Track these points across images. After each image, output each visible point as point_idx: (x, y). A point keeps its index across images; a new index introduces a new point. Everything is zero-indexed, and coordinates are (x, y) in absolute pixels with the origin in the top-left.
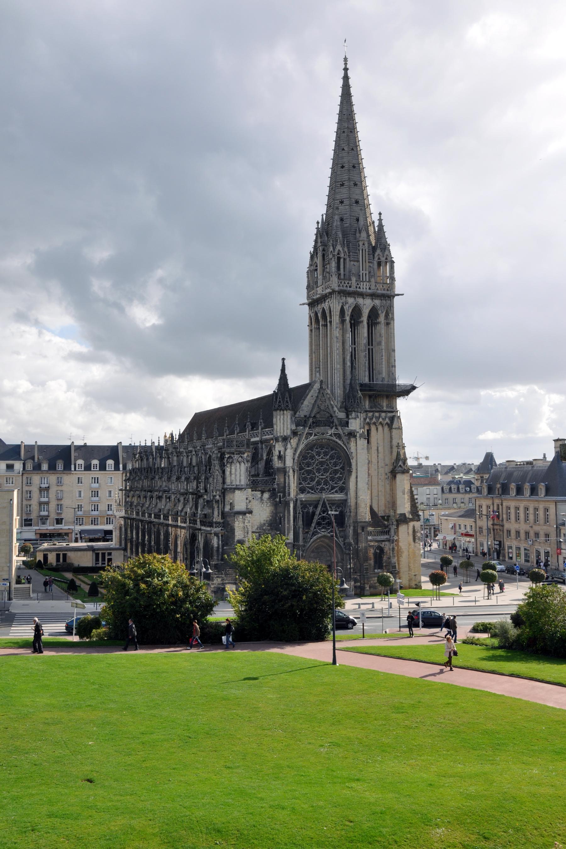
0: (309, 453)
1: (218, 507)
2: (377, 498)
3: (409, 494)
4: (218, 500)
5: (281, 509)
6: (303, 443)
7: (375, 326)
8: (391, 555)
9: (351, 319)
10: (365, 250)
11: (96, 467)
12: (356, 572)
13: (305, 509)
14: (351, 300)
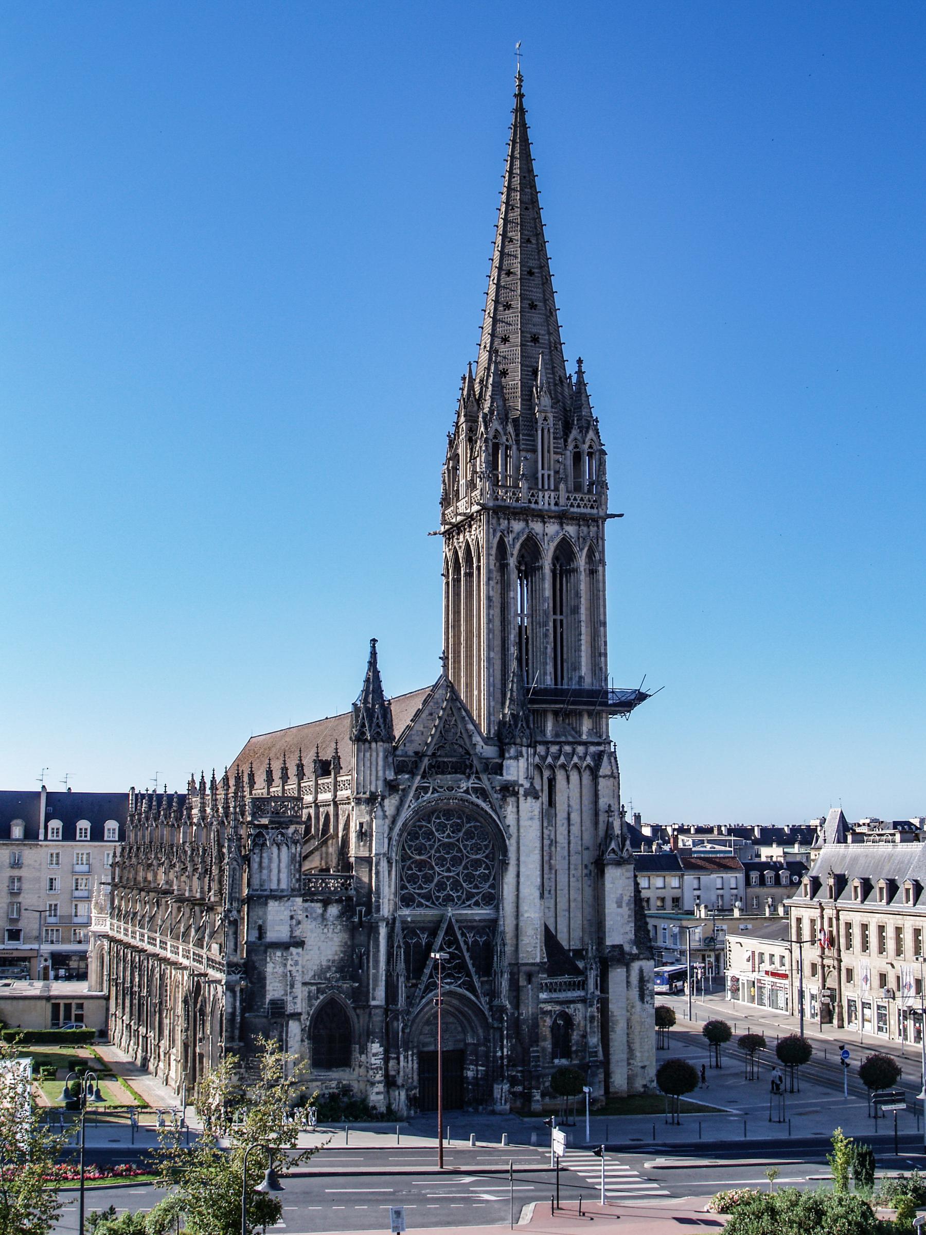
0: (422, 826)
2: (567, 913)
3: (633, 906)
5: (362, 938)
6: (409, 806)
7: (566, 576)
8: (588, 1030)
9: (519, 562)
10: (549, 430)
11: (86, 833)
12: (514, 1066)
13: (412, 939)
14: (517, 526)
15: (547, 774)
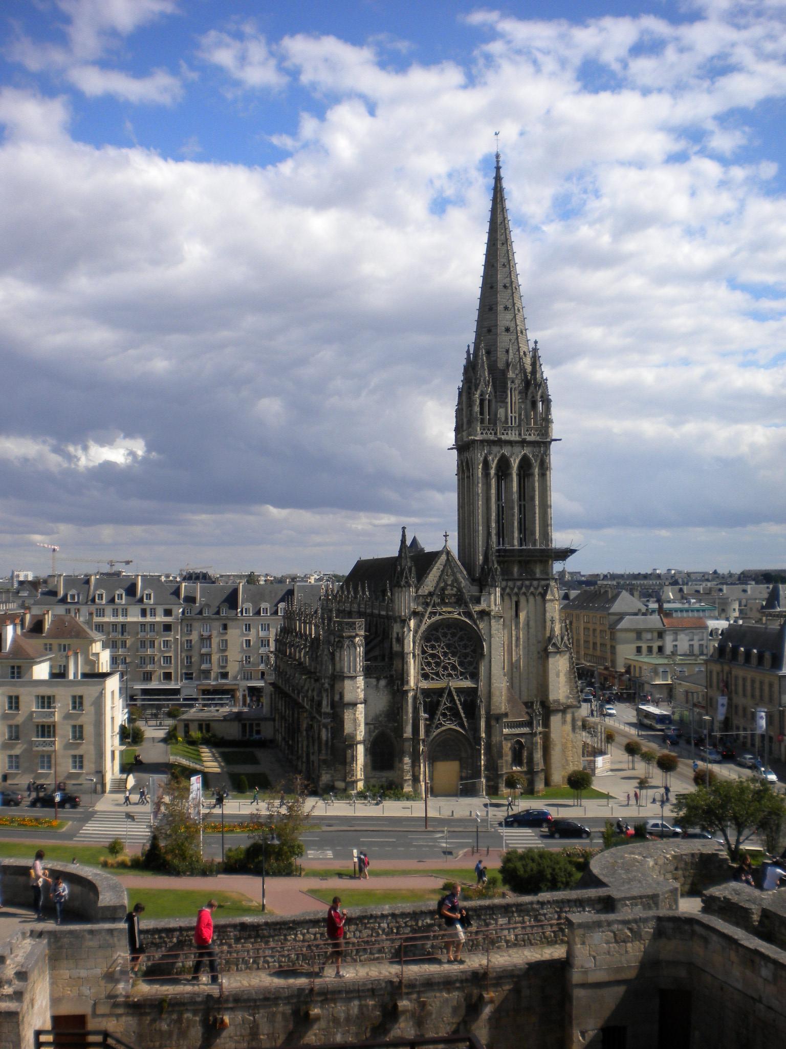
1: (327, 696)
4: (327, 690)
14: (495, 449)
15: (514, 599)
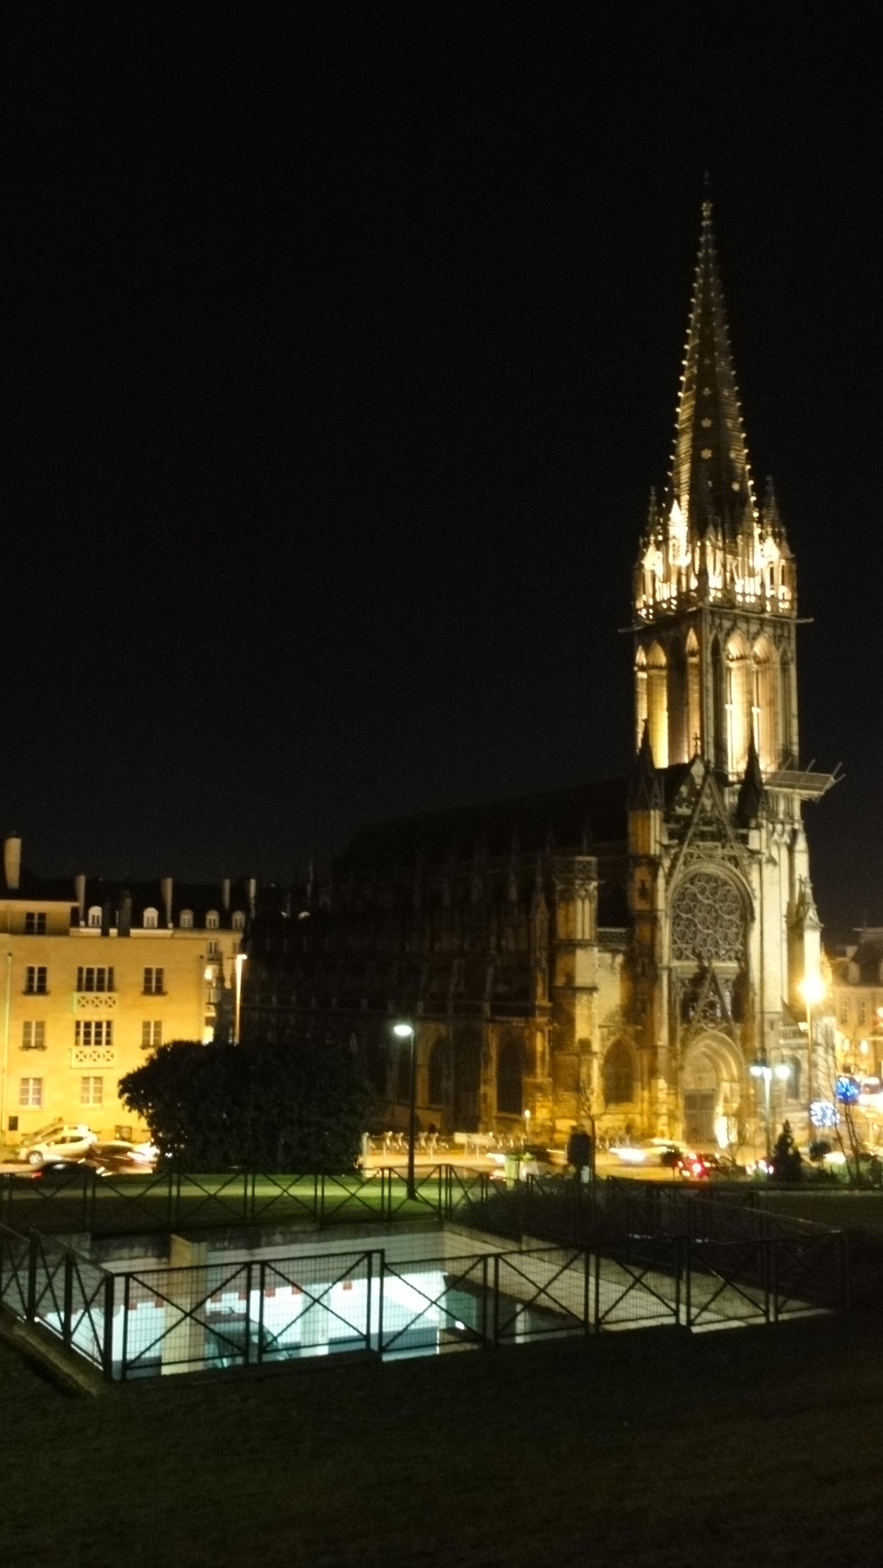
1: (544, 980)
4: (545, 969)
